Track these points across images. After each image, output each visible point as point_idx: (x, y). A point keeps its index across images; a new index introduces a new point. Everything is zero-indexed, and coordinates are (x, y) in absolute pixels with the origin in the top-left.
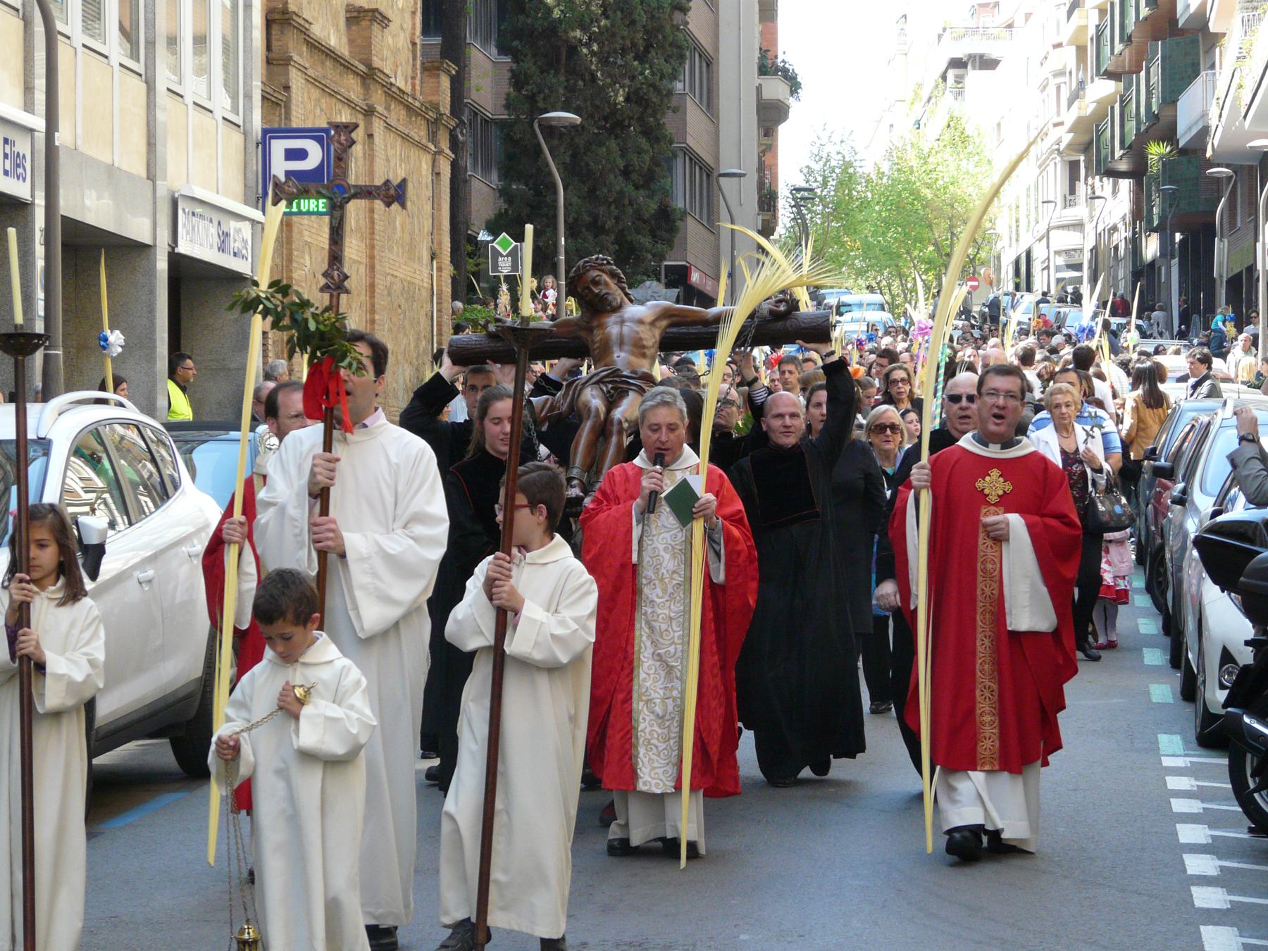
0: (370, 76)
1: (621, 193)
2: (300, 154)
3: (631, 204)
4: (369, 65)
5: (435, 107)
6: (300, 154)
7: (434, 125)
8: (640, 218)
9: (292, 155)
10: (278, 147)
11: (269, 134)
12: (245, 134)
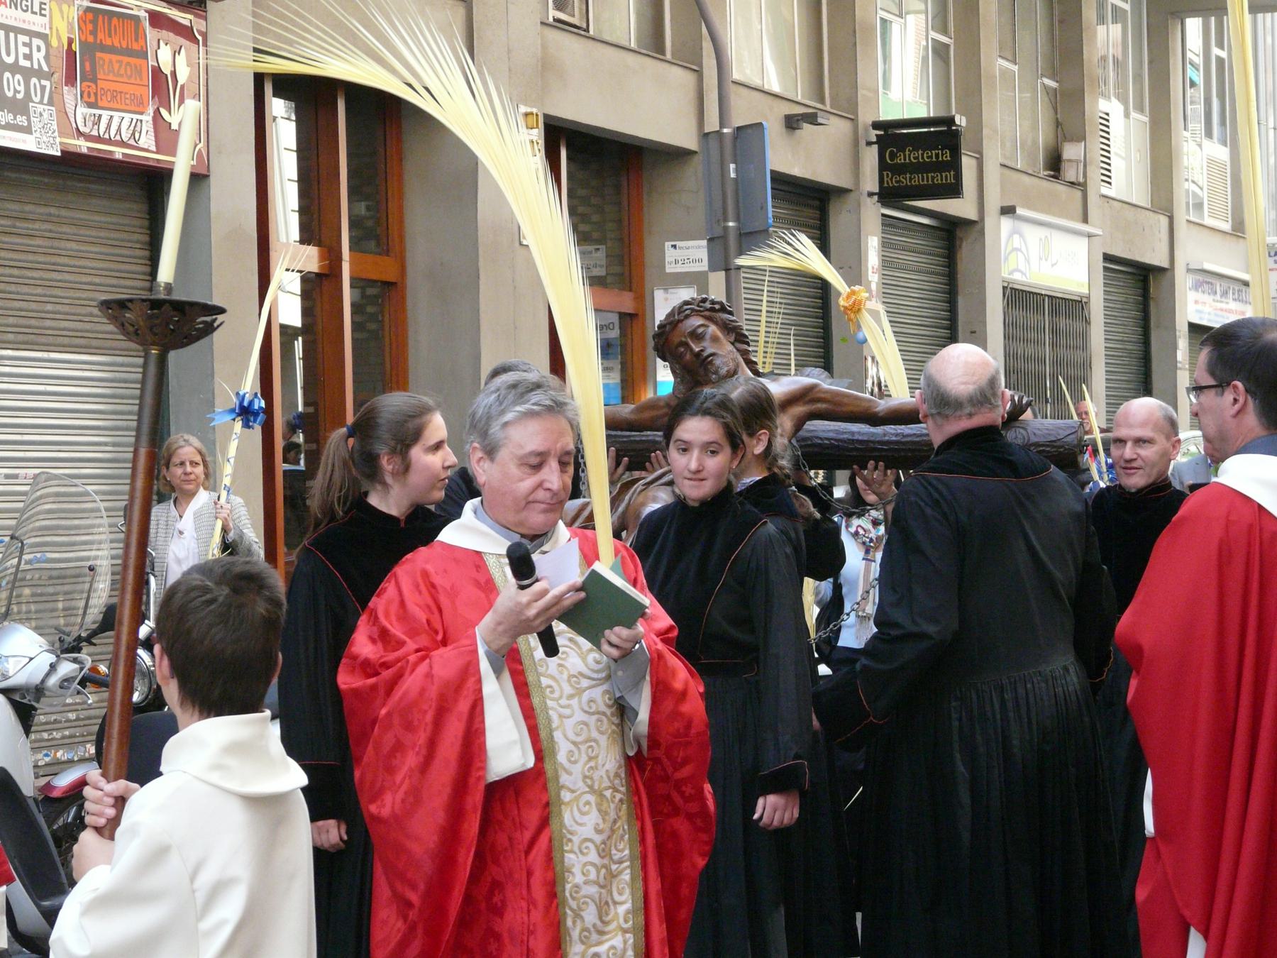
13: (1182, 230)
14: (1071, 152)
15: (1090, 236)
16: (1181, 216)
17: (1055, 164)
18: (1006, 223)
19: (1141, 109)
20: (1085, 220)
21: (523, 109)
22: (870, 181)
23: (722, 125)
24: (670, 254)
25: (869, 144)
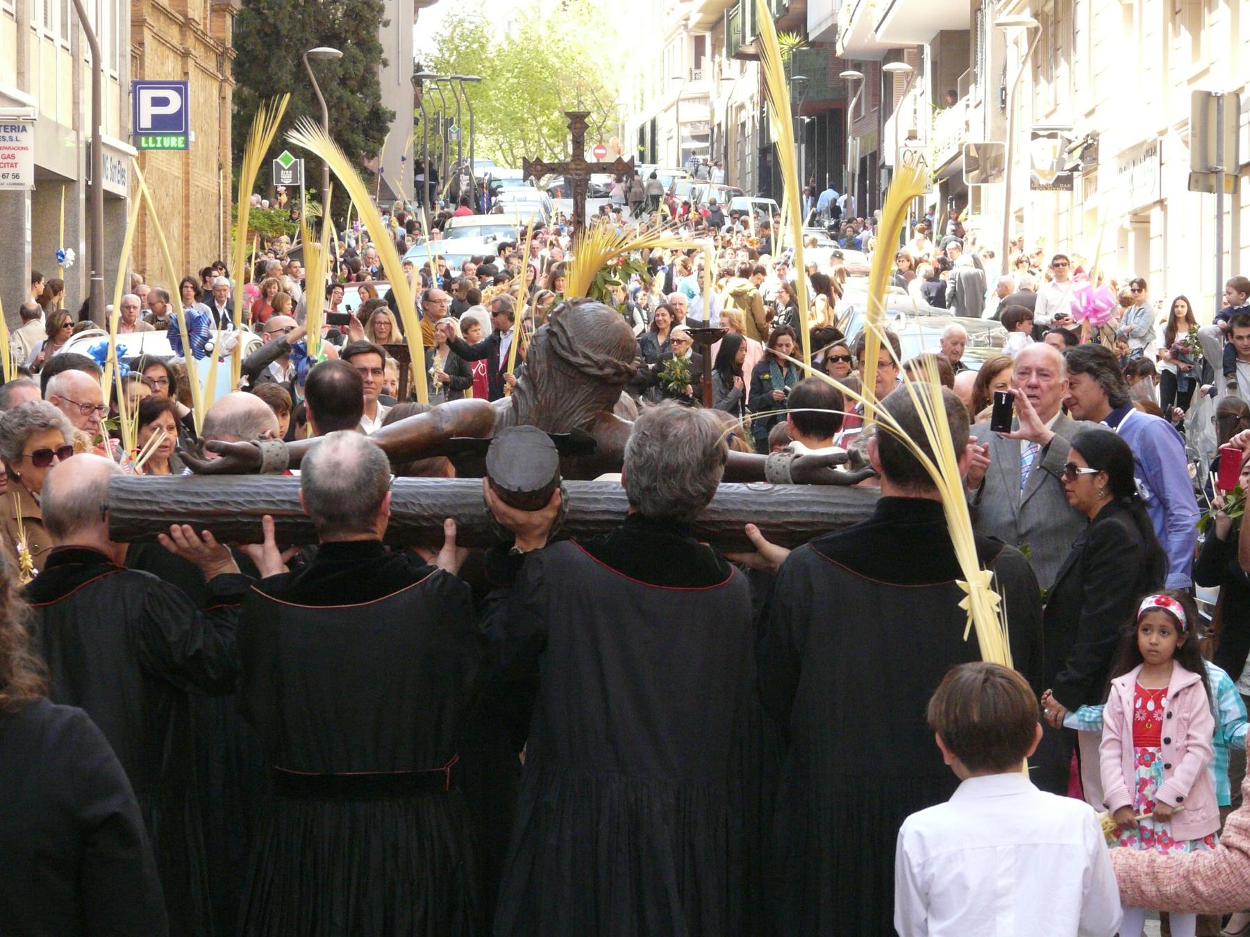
0: (186, 25)
1: (340, 98)
2: (164, 102)
3: (348, 108)
4: (185, 16)
5: (221, 42)
6: (164, 102)
7: (221, 56)
8: (354, 118)
9: (157, 102)
10: (146, 96)
11: (139, 84)
12: (120, 86)
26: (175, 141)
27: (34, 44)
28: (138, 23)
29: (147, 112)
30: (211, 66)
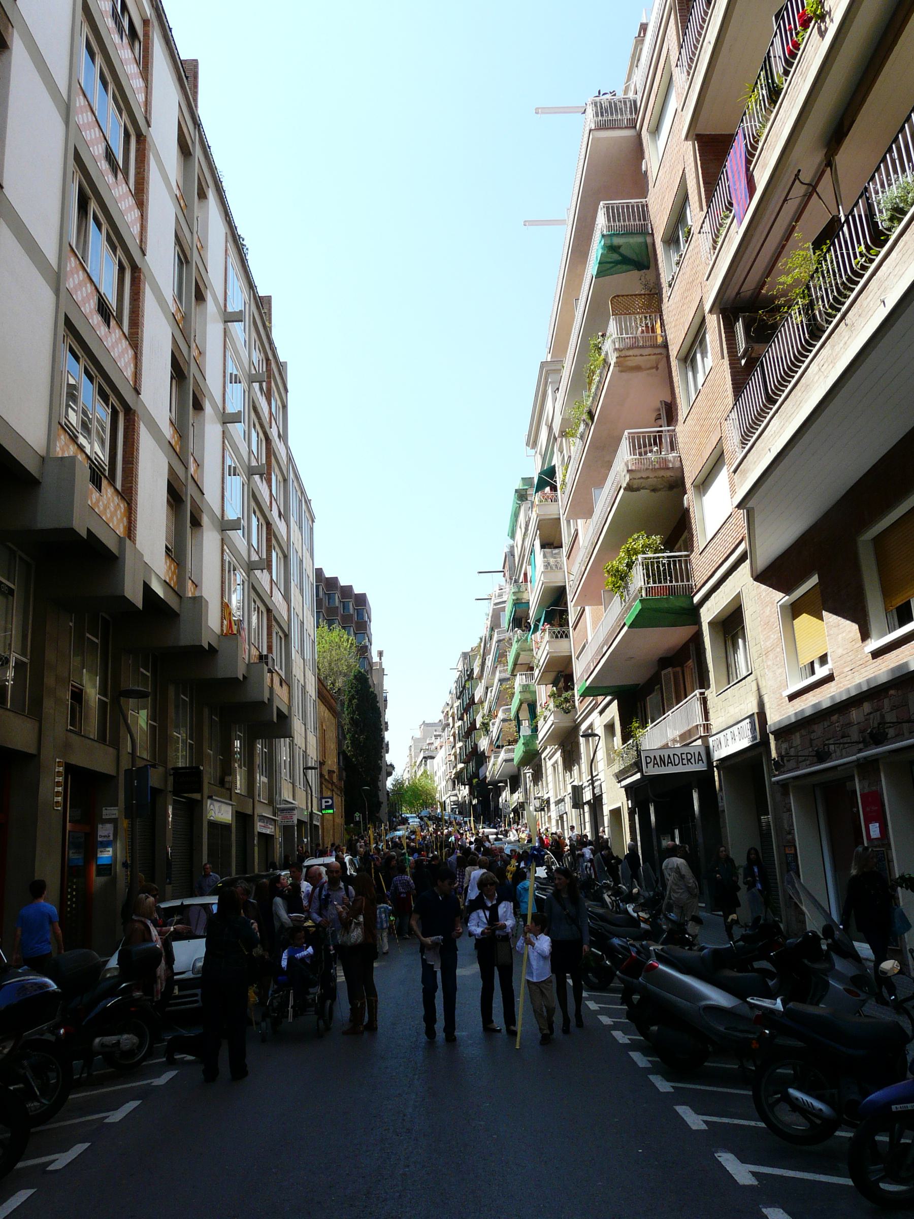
0: (333, 784)
2: (328, 802)
6: (328, 802)
9: (326, 802)
10: (324, 801)
11: (322, 798)
13: (256, 802)
14: (228, 779)
15: (232, 805)
16: (257, 798)
17: (222, 783)
18: (209, 802)
19: (245, 766)
20: (231, 800)
21: (58, 760)
22: (170, 788)
23: (133, 767)
24: (104, 812)
25: (170, 775)
26: (331, 811)
27: (297, 789)
28: (321, 784)
29: (324, 804)
30: (339, 793)
